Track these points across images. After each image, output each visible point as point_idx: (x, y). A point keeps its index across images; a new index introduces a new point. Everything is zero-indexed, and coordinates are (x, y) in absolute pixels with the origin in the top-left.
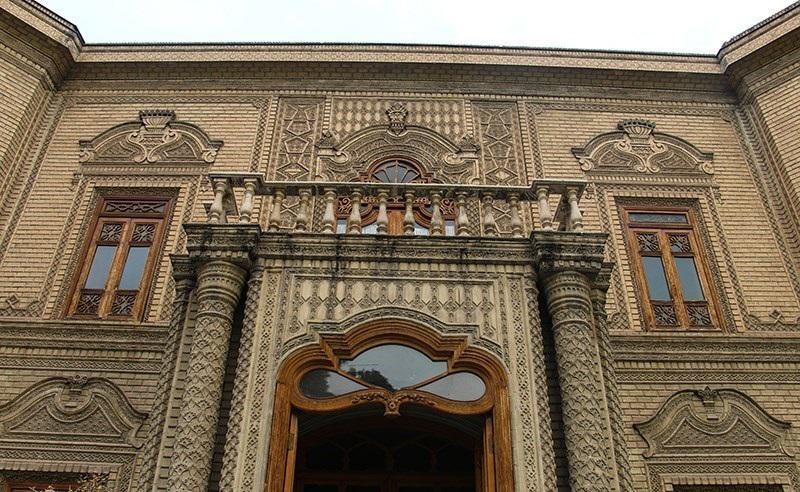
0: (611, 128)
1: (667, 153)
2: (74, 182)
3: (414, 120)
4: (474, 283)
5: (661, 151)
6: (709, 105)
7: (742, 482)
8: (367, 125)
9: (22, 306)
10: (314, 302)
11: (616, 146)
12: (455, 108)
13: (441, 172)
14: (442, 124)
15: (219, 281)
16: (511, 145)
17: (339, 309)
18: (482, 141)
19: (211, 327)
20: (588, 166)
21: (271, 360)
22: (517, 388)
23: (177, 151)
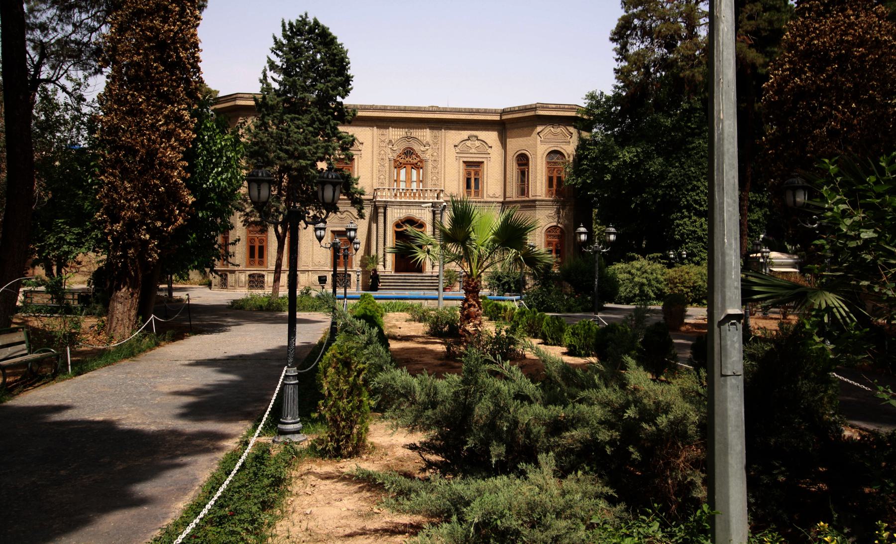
0: (466, 138)
18: (431, 143)
20: (458, 151)
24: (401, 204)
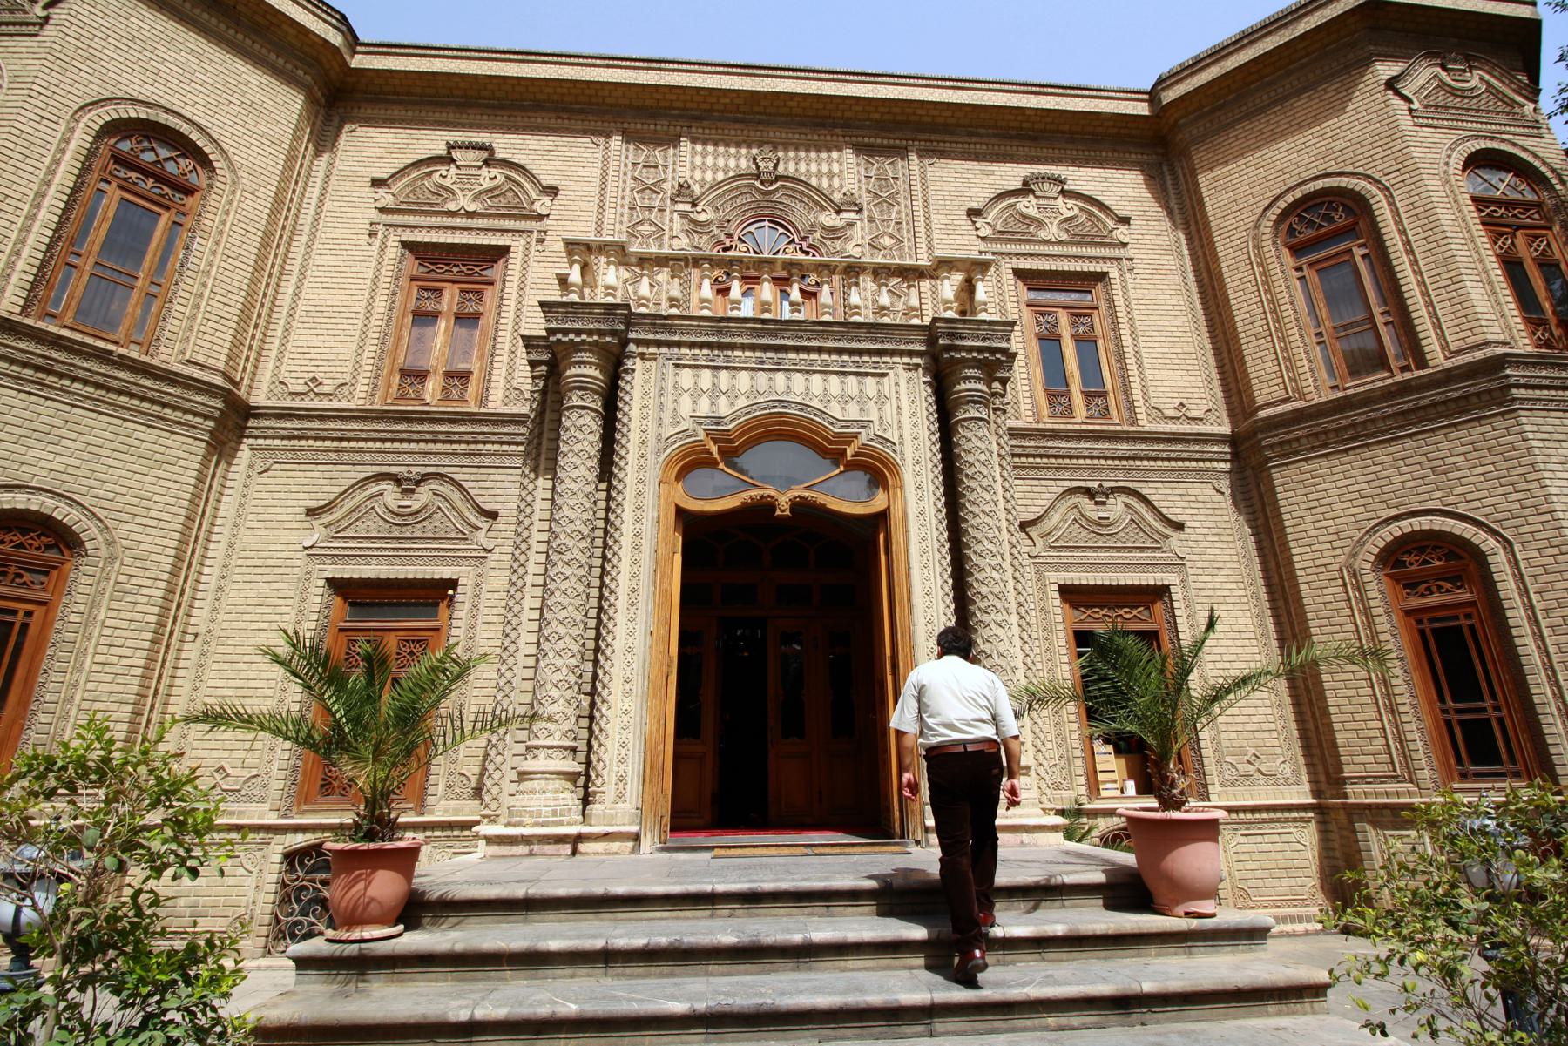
1: (1076, 216)
2: (372, 234)
3: (786, 169)
4: (867, 374)
5: (1071, 214)
6: (1133, 156)
7: (1130, 583)
8: (731, 174)
9: (326, 389)
10: (696, 393)
11: (1019, 206)
13: (817, 235)
14: (819, 175)
15: (587, 370)
16: (898, 203)
17: (723, 401)
18: (865, 199)
19: (581, 422)
21: (651, 458)
22: (913, 487)
23: (501, 199)
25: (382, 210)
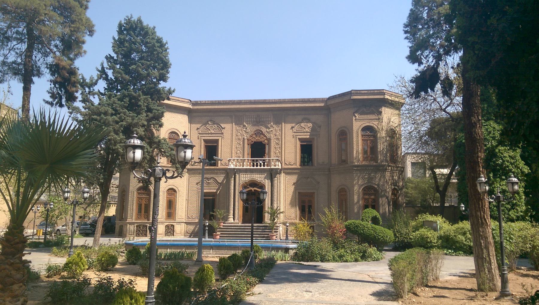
5: (310, 126)
12: (270, 116)
20: (295, 131)
24: (246, 171)
25: (200, 134)
